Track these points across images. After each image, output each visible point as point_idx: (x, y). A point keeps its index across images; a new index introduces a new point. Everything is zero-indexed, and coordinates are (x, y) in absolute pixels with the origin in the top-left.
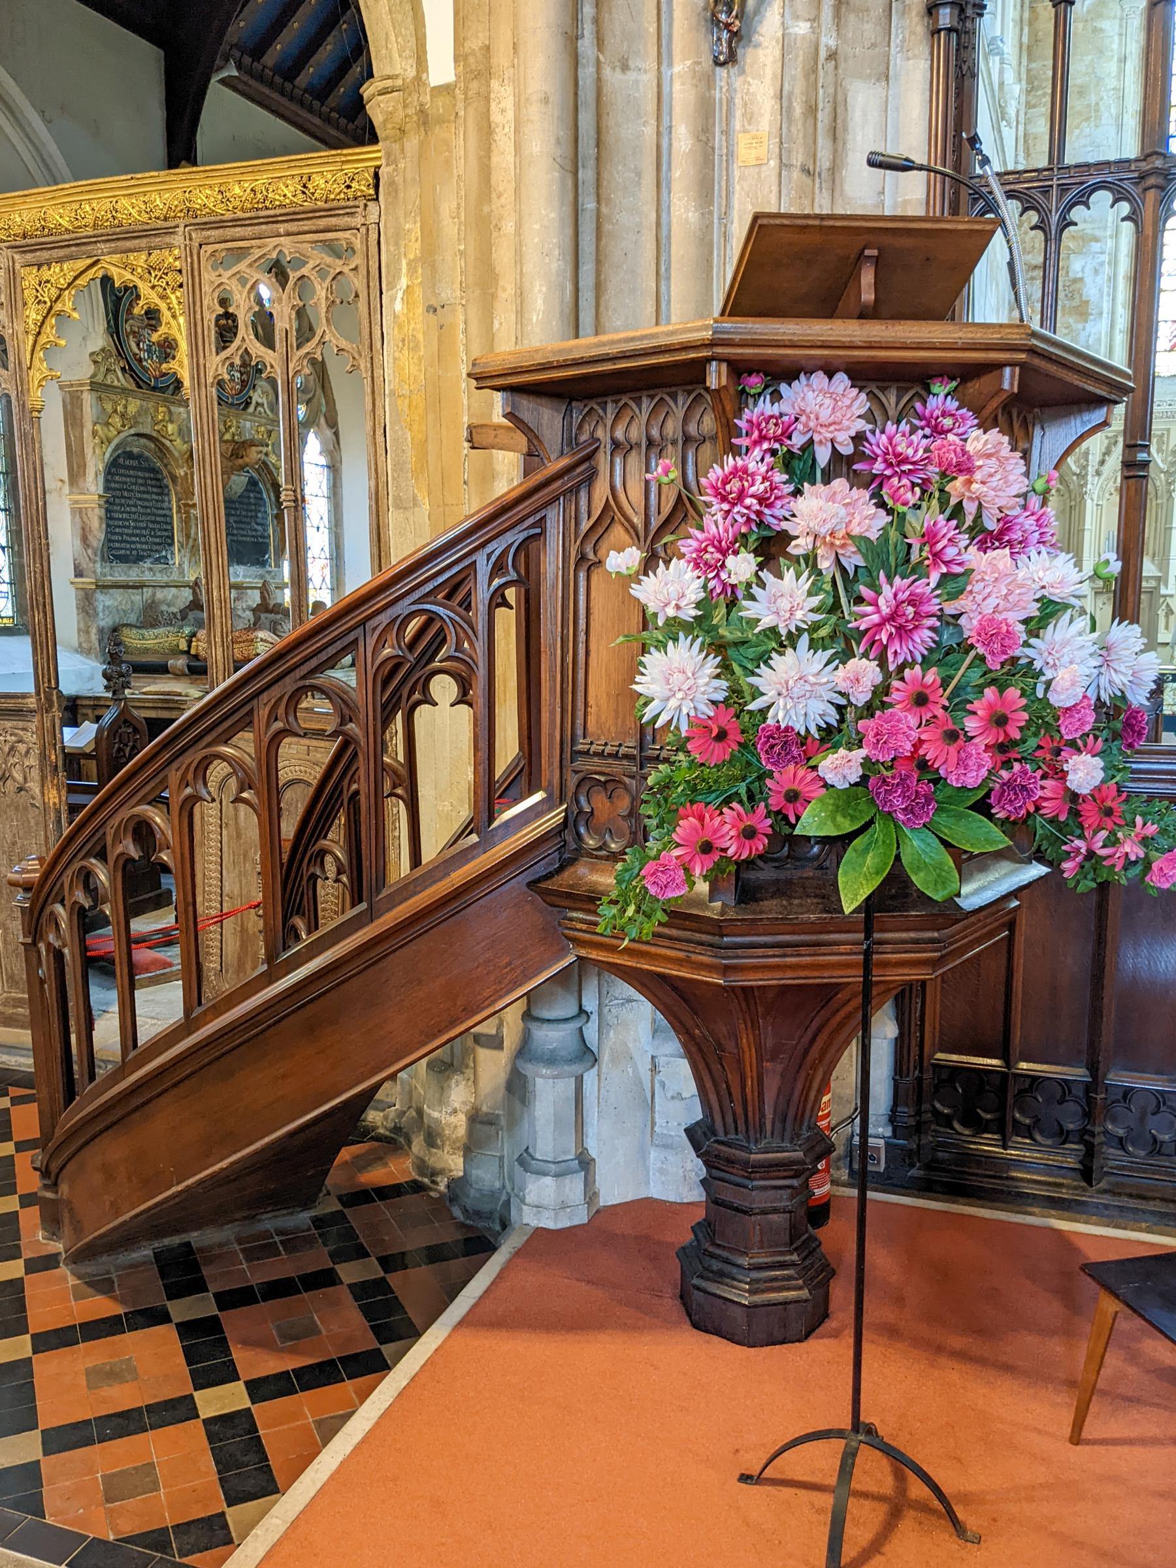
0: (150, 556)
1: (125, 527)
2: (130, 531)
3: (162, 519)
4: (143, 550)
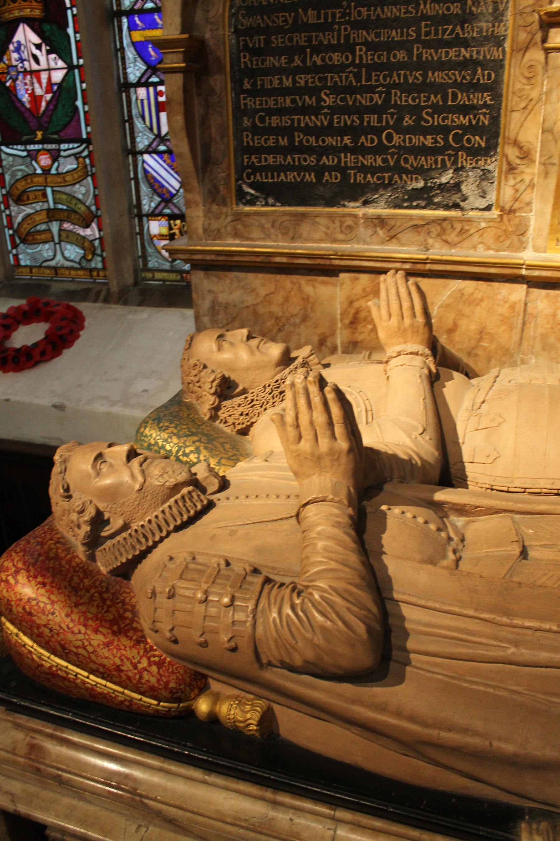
0: (385, 187)
1: (305, 111)
2: (322, 121)
4: (364, 169)
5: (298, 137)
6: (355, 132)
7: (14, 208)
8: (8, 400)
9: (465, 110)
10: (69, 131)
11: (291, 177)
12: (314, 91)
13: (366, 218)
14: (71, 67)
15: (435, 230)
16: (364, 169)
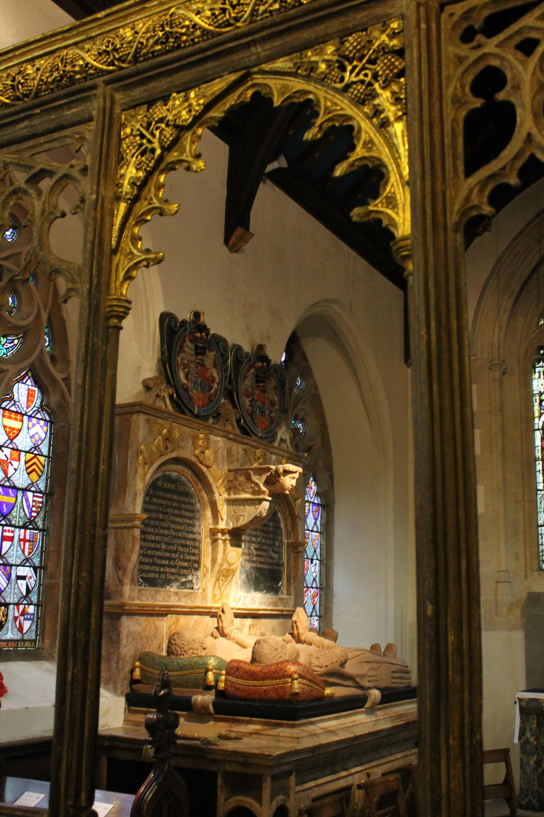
0: (176, 580)
2: (160, 554)
4: (172, 574)
5: (155, 559)
6: (170, 559)
8: (27, 708)
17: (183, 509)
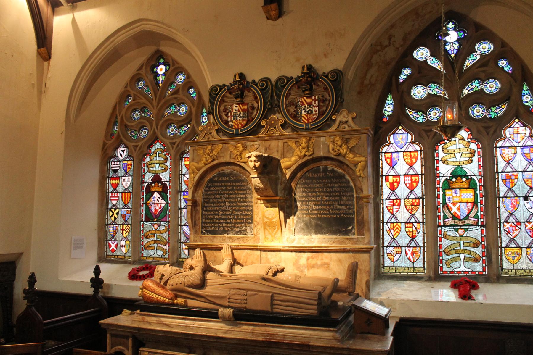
1: (216, 215)
3: (245, 208)
4: (227, 227)
5: (215, 220)
6: (226, 219)
7: (145, 239)
9: (247, 215)
10: (164, 219)
11: (213, 228)
12: (218, 211)
13: (228, 237)
14: (167, 203)
15: (241, 239)
16: (227, 227)
17: (236, 190)
